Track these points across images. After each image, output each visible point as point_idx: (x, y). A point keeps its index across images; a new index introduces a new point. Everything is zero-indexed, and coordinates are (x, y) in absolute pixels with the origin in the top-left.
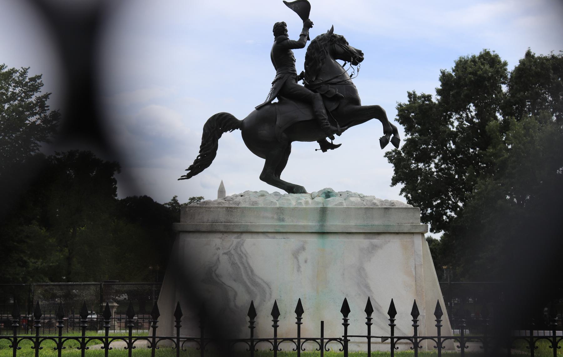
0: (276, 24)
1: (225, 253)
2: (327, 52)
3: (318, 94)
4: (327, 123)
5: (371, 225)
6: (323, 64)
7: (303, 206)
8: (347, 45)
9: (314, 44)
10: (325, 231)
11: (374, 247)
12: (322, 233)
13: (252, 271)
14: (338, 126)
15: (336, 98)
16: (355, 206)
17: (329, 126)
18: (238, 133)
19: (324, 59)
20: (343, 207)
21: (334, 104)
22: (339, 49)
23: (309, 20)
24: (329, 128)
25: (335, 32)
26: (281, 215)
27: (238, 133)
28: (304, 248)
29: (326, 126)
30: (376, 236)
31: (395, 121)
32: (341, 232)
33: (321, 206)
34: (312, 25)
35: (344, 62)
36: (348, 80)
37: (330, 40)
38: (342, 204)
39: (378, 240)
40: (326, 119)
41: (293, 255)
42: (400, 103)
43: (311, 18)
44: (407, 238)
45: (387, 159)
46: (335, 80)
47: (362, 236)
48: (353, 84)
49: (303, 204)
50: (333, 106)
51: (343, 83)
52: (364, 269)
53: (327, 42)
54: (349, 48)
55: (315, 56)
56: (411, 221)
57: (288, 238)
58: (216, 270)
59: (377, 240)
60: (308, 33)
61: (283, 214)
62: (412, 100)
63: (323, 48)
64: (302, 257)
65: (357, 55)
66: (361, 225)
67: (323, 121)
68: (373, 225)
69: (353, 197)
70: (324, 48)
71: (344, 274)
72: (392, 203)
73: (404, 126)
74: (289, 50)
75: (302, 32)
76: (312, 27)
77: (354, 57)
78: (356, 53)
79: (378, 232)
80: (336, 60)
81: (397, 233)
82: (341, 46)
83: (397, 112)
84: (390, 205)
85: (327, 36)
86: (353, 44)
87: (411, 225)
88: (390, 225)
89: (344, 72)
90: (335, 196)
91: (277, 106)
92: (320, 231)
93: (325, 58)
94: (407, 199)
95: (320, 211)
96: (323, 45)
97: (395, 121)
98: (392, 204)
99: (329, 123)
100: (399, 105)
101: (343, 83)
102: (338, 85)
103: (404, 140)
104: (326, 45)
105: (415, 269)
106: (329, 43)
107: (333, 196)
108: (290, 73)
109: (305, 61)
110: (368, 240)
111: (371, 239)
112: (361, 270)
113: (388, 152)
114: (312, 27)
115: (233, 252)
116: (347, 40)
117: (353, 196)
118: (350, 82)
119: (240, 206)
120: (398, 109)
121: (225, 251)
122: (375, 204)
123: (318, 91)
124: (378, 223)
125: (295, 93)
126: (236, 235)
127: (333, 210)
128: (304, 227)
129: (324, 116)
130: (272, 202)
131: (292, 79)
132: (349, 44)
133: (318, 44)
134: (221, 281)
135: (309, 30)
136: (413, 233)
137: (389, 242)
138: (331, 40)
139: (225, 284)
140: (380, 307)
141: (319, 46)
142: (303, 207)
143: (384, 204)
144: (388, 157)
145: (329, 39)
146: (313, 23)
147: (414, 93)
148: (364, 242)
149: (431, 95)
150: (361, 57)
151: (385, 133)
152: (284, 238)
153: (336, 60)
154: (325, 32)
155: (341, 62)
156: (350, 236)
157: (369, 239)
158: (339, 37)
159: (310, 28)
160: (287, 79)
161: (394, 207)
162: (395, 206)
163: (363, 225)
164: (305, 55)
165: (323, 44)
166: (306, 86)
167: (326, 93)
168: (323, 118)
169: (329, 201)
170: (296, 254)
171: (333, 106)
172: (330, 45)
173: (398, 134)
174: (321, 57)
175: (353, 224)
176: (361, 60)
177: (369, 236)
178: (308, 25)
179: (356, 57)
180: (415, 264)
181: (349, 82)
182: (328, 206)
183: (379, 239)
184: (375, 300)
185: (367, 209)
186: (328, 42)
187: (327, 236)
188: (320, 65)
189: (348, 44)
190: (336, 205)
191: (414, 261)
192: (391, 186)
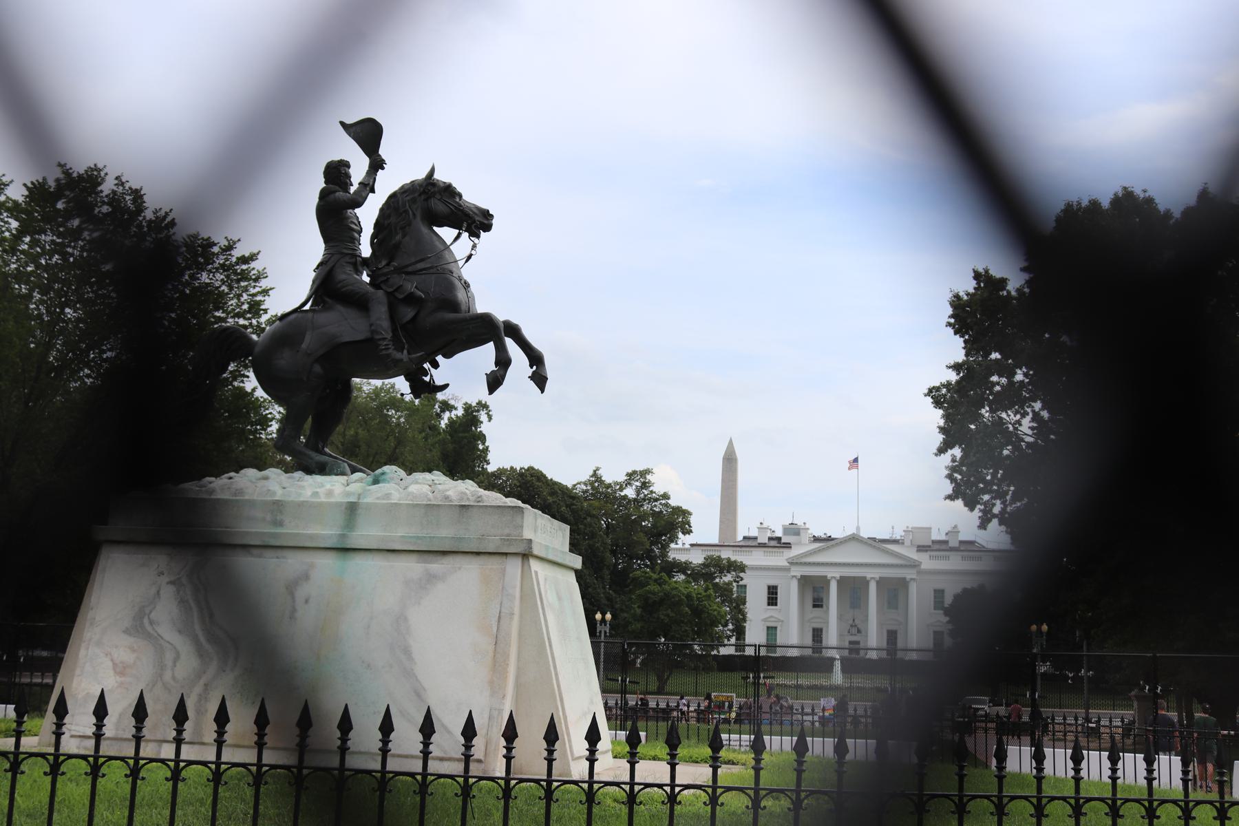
0: (328, 163)
2: (414, 214)
3: (380, 293)
4: (386, 347)
5: (430, 537)
6: (404, 236)
7: (320, 498)
8: (458, 200)
9: (393, 200)
10: (348, 547)
11: (431, 578)
14: (405, 352)
15: (411, 299)
16: (412, 501)
17: (390, 351)
19: (407, 228)
20: (390, 501)
21: (409, 310)
22: (438, 206)
23: (380, 156)
24: (388, 356)
25: (437, 176)
26: (278, 514)
28: (307, 577)
29: (384, 352)
30: (439, 558)
31: (947, 326)
32: (375, 548)
33: (352, 499)
34: (384, 165)
35: (458, 231)
36: (443, 266)
37: (424, 190)
38: (388, 497)
39: (443, 566)
40: (384, 339)
41: (287, 588)
42: (956, 291)
43: (383, 151)
44: (494, 563)
45: (929, 400)
46: (420, 266)
47: (414, 557)
48: (452, 273)
49: (322, 495)
50: (408, 313)
51: (434, 270)
52: (406, 619)
53: (416, 195)
54: (461, 206)
55: (389, 222)
56: (507, 531)
57: (284, 557)
58: (151, 612)
59: (438, 566)
60: (372, 180)
61: (281, 512)
62: (982, 285)
63: (408, 207)
65: (477, 218)
66: (411, 537)
67: (381, 342)
68: (434, 537)
69: (420, 483)
70: (410, 207)
71: (369, 627)
72: (479, 497)
73: (962, 336)
74: (344, 211)
75: (365, 178)
76: (383, 168)
77: (469, 221)
78: (476, 214)
79: (442, 550)
80: (435, 228)
81: (478, 553)
82: (445, 203)
83: (950, 311)
84: (476, 501)
85: (418, 184)
86: (472, 195)
87: (501, 539)
88: (464, 538)
89: (442, 248)
90: (389, 482)
91: (310, 315)
92: (339, 546)
93: (410, 225)
94: (951, 483)
95: (346, 508)
96: (408, 201)
97: (947, 326)
98: (480, 499)
99: (390, 346)
100: (954, 297)
101: (434, 270)
102: (423, 276)
103: (947, 366)
104: (414, 201)
105: (499, 622)
106: (423, 197)
107: (384, 481)
108: (342, 253)
109: (372, 231)
110: (423, 565)
111: (429, 563)
113: (934, 387)
114: (383, 168)
116: (459, 189)
117: (420, 481)
118: (447, 269)
119: (212, 497)
120: (953, 304)
122: (447, 498)
123: (383, 286)
124: (445, 533)
125: (344, 289)
127: (369, 507)
128: (312, 537)
129: (383, 333)
130: (269, 490)
131: (345, 264)
132: (464, 198)
133: (400, 199)
134: (156, 632)
135: (378, 174)
136: (506, 554)
137: (460, 568)
138: (427, 191)
139: (162, 638)
140: (425, 690)
141: (400, 203)
142: (319, 500)
143: (465, 498)
144: (932, 397)
145: (422, 189)
146: (386, 162)
147: (987, 271)
148: (413, 567)
149: (1006, 279)
150: (486, 222)
151: (497, 364)
152: (278, 558)
153: (435, 228)
154: (421, 175)
155: (446, 233)
156: (392, 556)
157: (425, 563)
158: (442, 185)
159: (380, 170)
160: (334, 266)
161: (481, 504)
162: (483, 502)
163: (414, 537)
164: (374, 221)
165: (408, 198)
167: (396, 290)
168: (381, 337)
169: (369, 490)
171: (408, 313)
172: (424, 200)
173: (544, 365)
174: (402, 223)
175: (400, 534)
176: (487, 228)
177: (426, 557)
178: (377, 164)
179: (474, 222)
180: (500, 612)
181: (444, 269)
182: (360, 501)
183: (443, 564)
184: (416, 677)
185: (430, 507)
186: (420, 195)
187: (352, 555)
188: (398, 237)
189: (460, 196)
190: (378, 498)
191: (498, 606)
192: (936, 455)
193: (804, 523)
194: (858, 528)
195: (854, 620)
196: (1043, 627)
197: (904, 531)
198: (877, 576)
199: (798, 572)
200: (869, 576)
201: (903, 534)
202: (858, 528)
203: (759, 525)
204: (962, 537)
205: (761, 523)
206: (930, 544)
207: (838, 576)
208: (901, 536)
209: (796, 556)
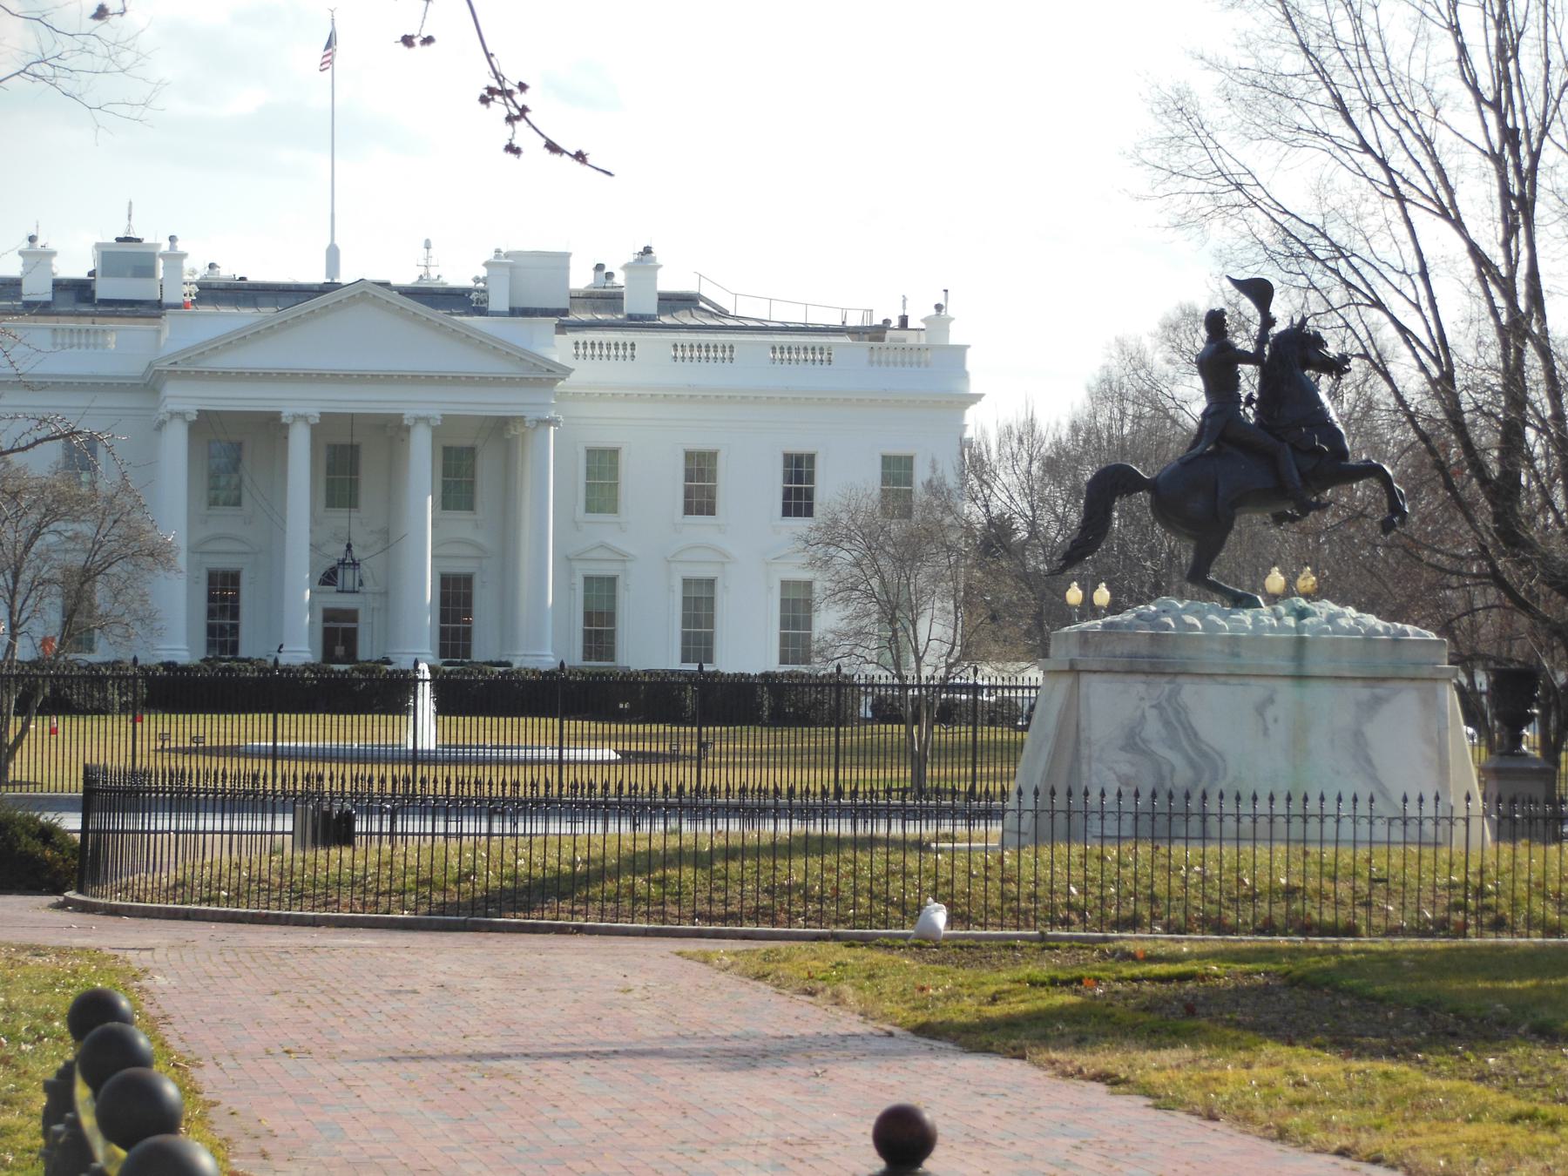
1: (1153, 707)
11: (1377, 701)
12: (1300, 677)
13: (1196, 734)
18: (1143, 497)
27: (1143, 497)
47: (1359, 683)
59: (1381, 690)
64: (1270, 713)
81: (1413, 679)
112: (1358, 736)
115: (1164, 704)
121: (1154, 703)
126: (1166, 679)
166: (1259, 423)
170: (1260, 710)
193: (172, 239)
194: (333, 254)
195: (349, 546)
196: (1069, 594)
197: (487, 264)
198: (435, 412)
199: (186, 398)
200: (409, 412)
201: (483, 273)
202: (333, 254)
203: (25, 245)
204: (669, 282)
205: (32, 239)
206: (564, 303)
207: (314, 411)
208: (477, 280)
209: (184, 351)
